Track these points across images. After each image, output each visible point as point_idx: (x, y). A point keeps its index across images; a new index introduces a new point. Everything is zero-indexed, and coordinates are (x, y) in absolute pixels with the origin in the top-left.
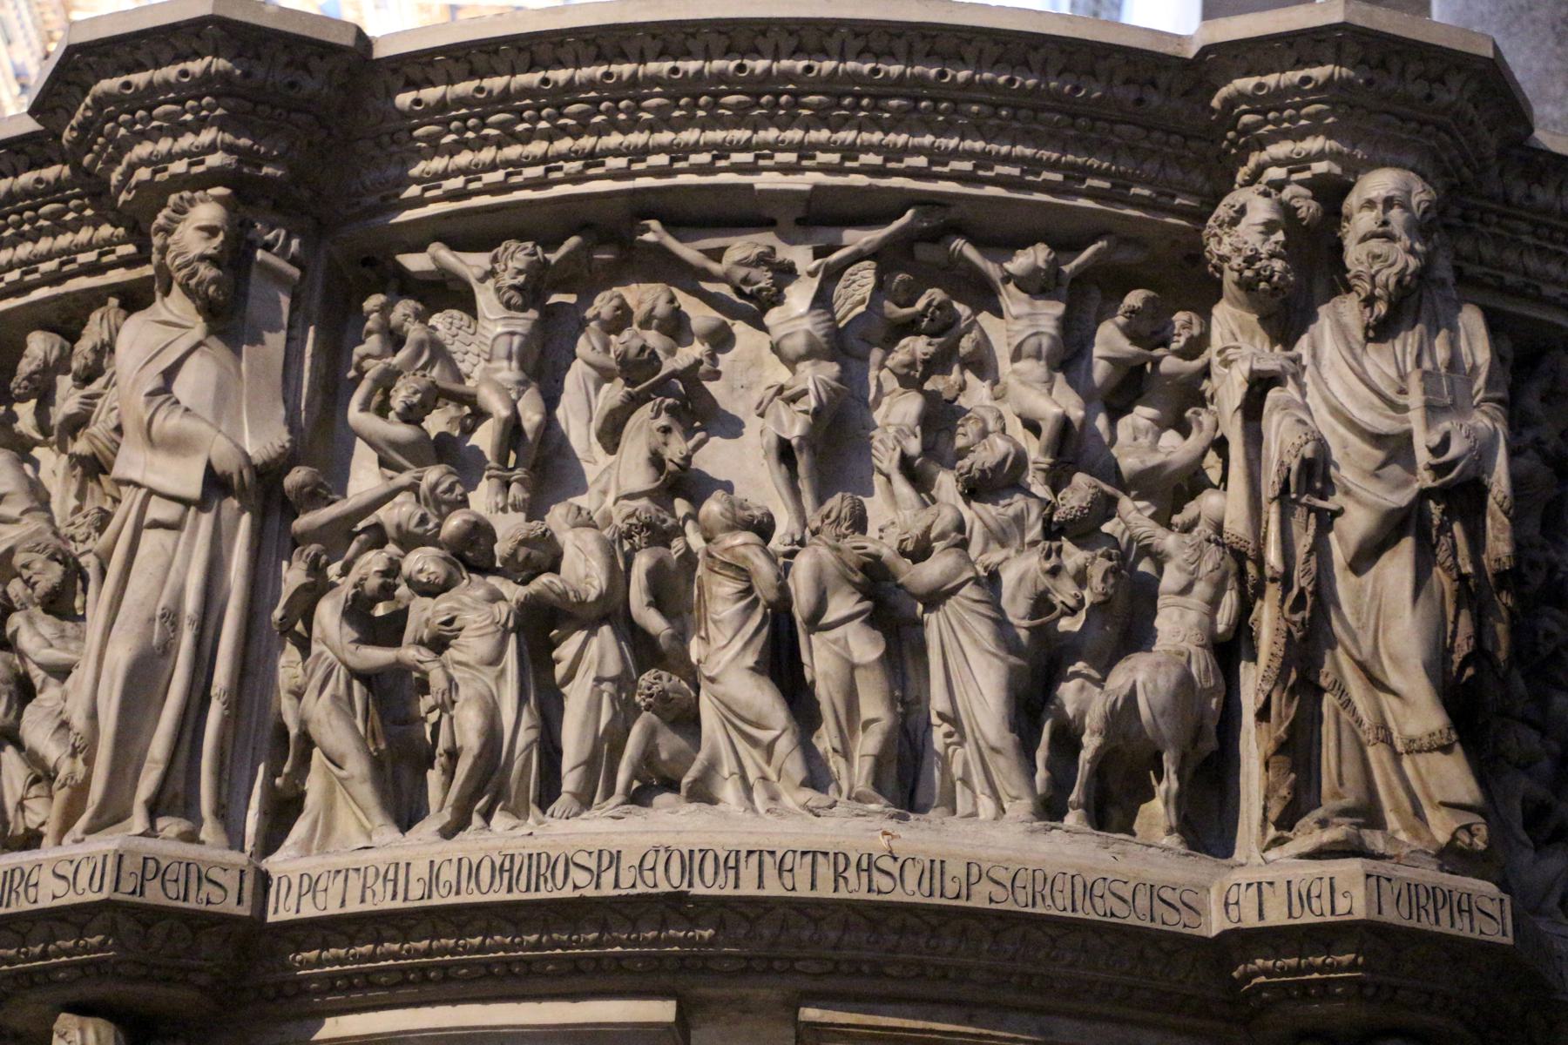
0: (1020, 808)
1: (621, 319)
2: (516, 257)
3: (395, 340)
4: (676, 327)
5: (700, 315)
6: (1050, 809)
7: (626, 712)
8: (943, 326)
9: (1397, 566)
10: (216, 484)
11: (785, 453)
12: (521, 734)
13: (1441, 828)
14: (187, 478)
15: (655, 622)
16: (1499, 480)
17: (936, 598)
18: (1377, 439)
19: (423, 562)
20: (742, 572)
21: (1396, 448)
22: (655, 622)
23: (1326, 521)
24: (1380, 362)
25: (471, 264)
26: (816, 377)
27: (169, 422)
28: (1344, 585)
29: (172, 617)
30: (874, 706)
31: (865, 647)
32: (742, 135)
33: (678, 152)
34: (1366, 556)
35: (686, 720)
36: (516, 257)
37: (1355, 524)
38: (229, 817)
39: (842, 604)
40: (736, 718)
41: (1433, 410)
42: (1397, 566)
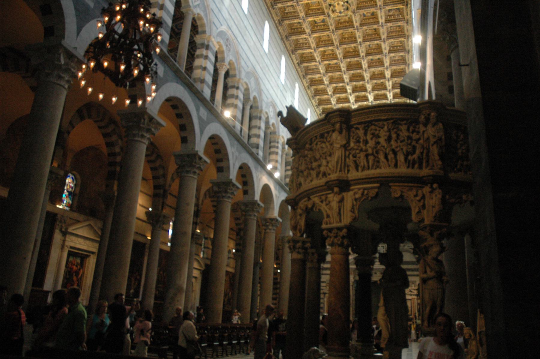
0: (406, 167)
1: (371, 130)
2: (363, 126)
3: (354, 133)
4: (376, 130)
5: (378, 129)
6: (408, 167)
7: (374, 162)
8: (397, 128)
9: (435, 146)
10: (341, 146)
11: (386, 140)
12: (366, 164)
13: (439, 167)
14: (339, 146)
15: (376, 155)
16: (443, 137)
17: (398, 151)
18: (433, 135)
19: (358, 151)
20: (382, 151)
21: (435, 136)
22: (376, 155)
23: (429, 142)
24: (433, 129)
25: (359, 126)
26: (387, 134)
27: (338, 141)
28: (431, 148)
29: (338, 157)
30: (394, 161)
31: (393, 156)
32: (380, 114)
33: (375, 116)
34: (432, 145)
35: (378, 162)
36: (363, 126)
37: (432, 143)
38: (344, 171)
39: (391, 153)
40: (382, 162)
41: (438, 132)
42: (435, 146)
